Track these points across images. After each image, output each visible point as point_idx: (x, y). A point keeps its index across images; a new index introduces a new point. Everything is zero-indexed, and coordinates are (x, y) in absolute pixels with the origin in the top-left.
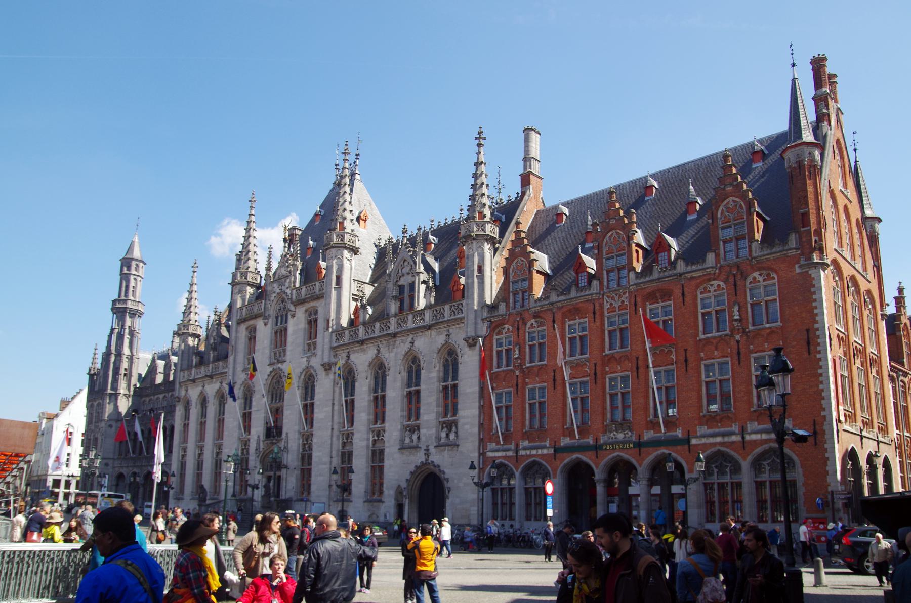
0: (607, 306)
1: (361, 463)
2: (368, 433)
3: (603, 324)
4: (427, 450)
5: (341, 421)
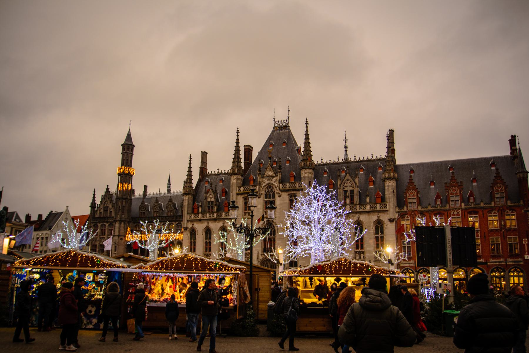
0: (452, 213)
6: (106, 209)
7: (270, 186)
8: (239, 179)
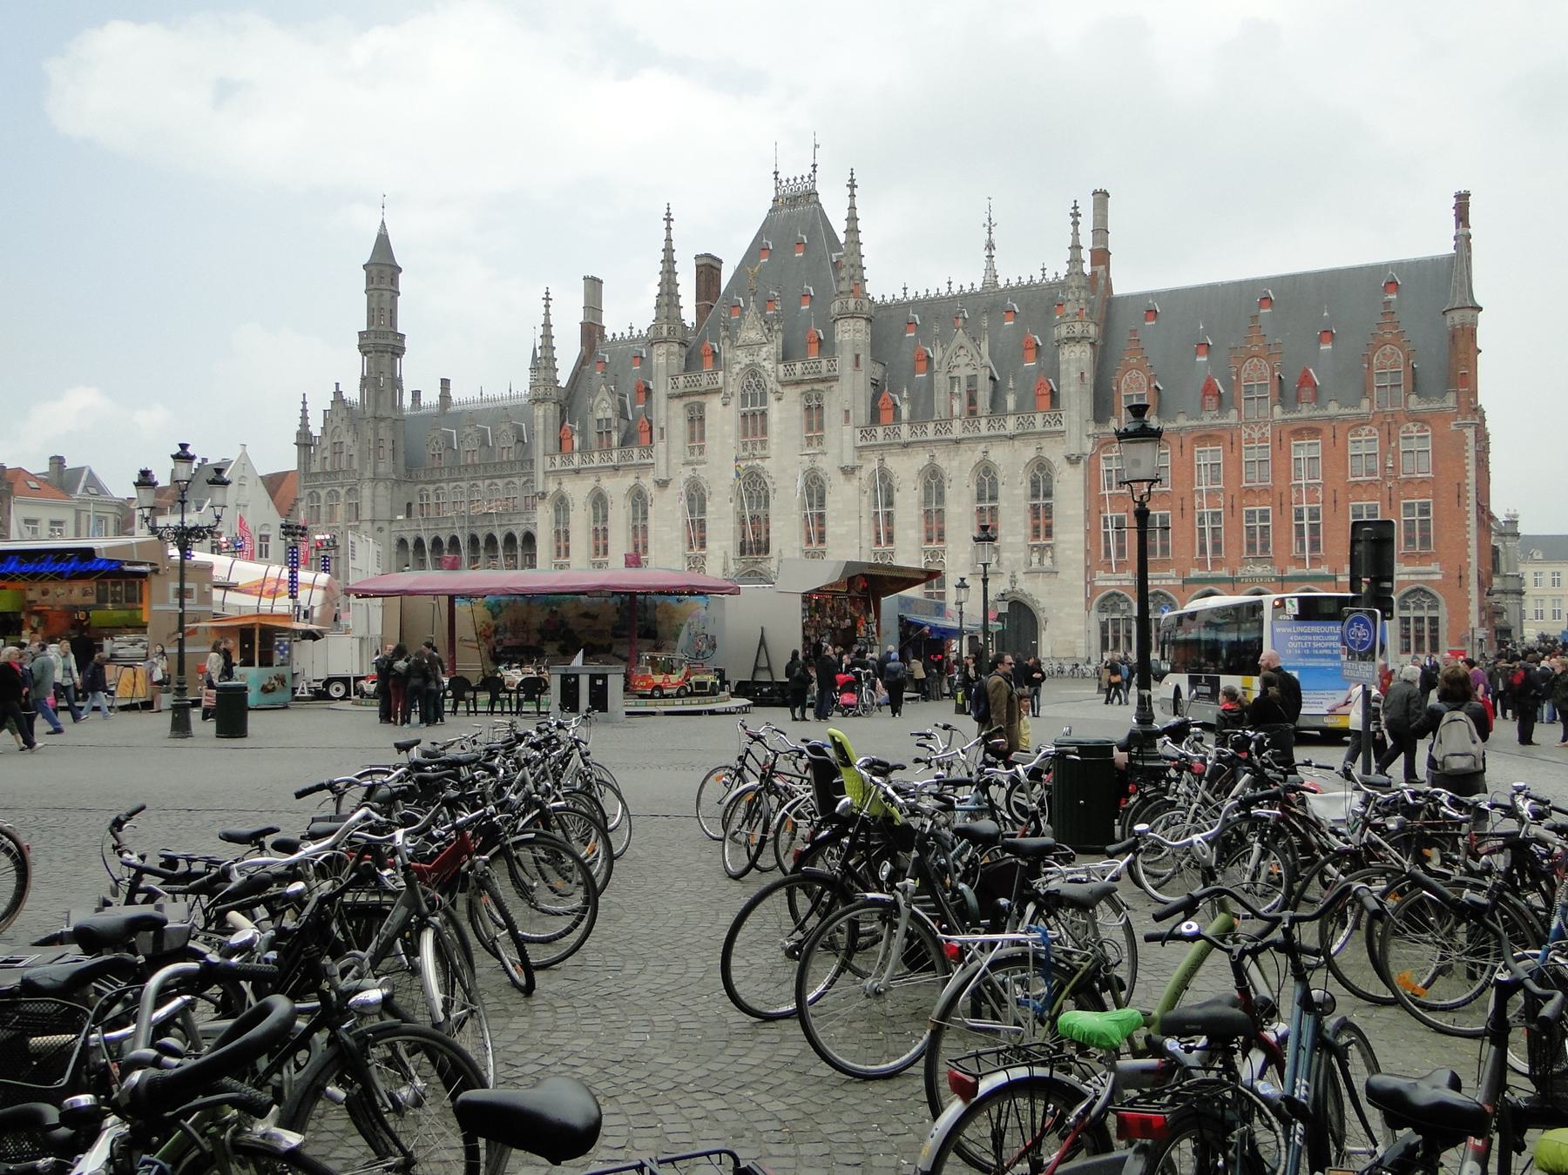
0: (1244, 436)
4: (1013, 576)
5: (873, 537)
6: (337, 449)
8: (673, 354)
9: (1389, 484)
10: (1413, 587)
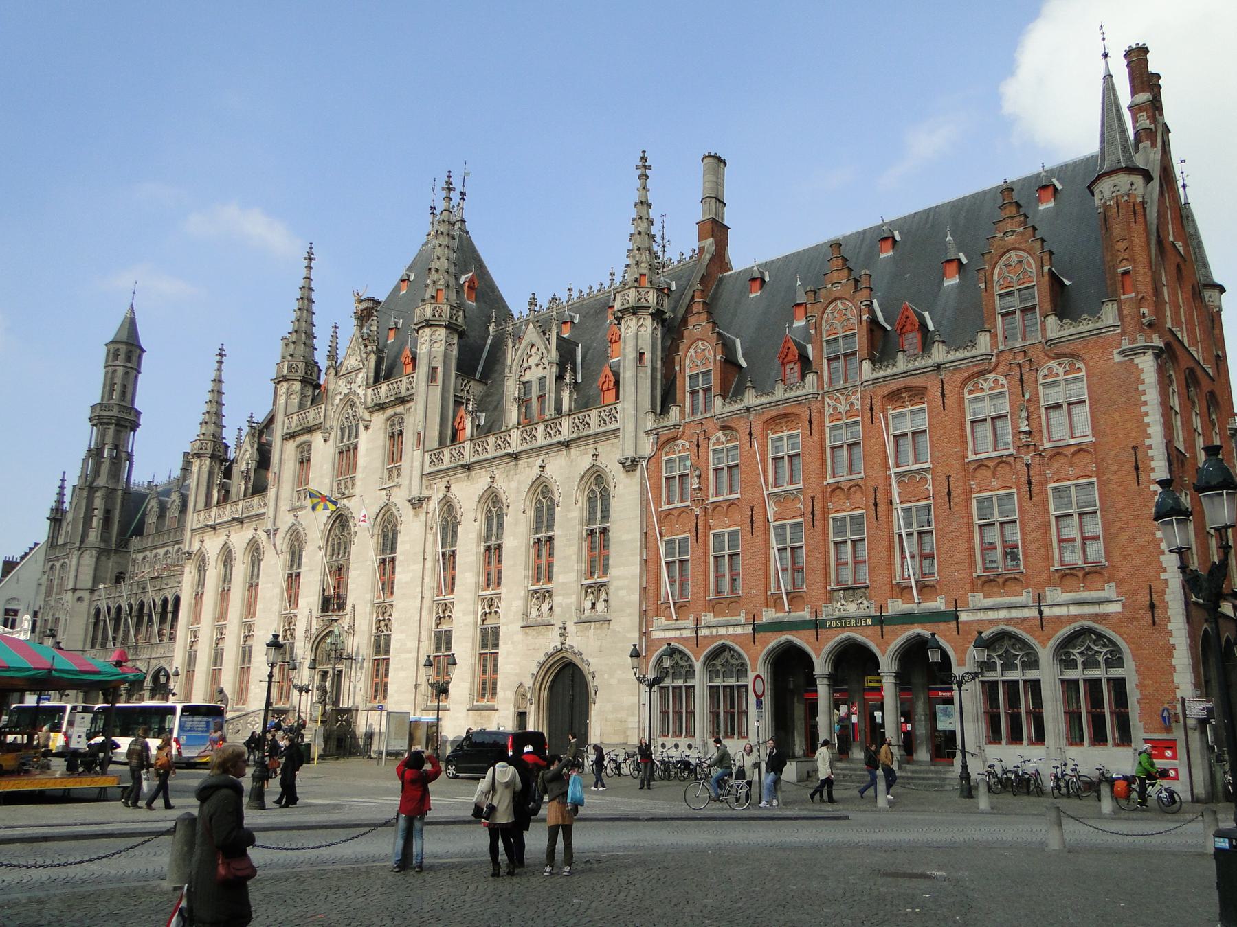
0: (828, 411)
1: (464, 648)
2: (476, 603)
3: (822, 439)
7: (349, 401)
9: (1027, 458)
10: (1076, 626)
